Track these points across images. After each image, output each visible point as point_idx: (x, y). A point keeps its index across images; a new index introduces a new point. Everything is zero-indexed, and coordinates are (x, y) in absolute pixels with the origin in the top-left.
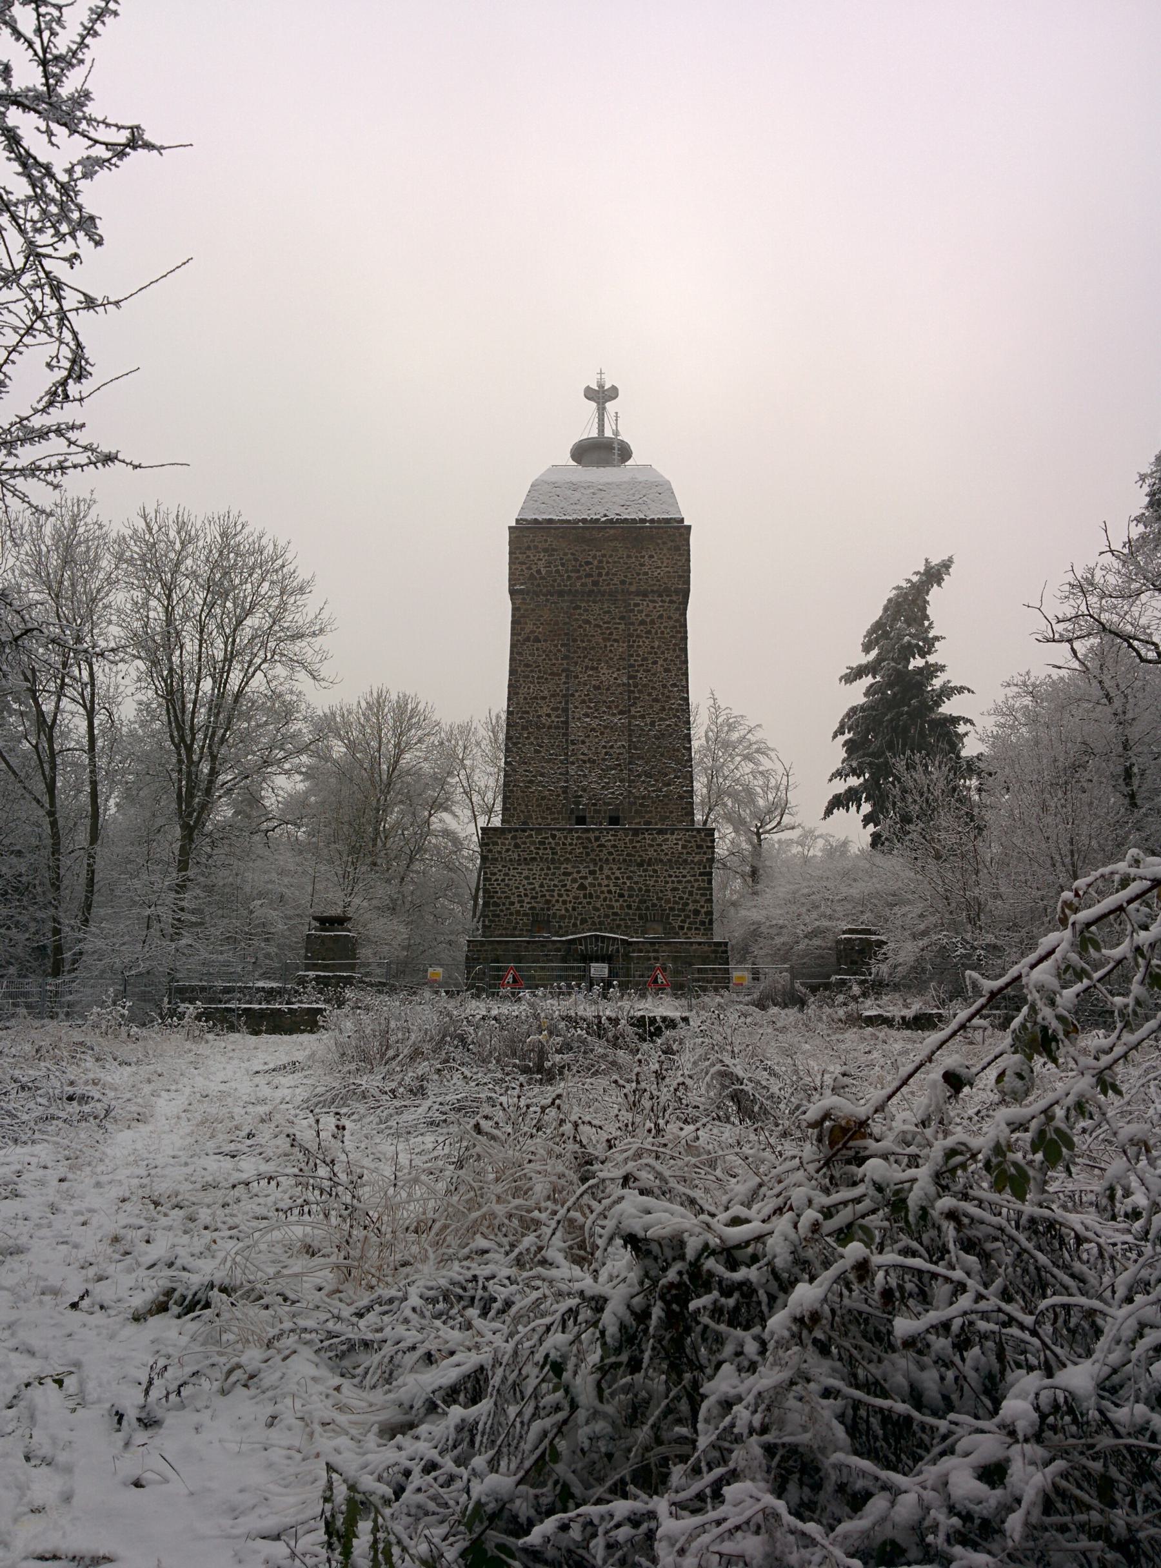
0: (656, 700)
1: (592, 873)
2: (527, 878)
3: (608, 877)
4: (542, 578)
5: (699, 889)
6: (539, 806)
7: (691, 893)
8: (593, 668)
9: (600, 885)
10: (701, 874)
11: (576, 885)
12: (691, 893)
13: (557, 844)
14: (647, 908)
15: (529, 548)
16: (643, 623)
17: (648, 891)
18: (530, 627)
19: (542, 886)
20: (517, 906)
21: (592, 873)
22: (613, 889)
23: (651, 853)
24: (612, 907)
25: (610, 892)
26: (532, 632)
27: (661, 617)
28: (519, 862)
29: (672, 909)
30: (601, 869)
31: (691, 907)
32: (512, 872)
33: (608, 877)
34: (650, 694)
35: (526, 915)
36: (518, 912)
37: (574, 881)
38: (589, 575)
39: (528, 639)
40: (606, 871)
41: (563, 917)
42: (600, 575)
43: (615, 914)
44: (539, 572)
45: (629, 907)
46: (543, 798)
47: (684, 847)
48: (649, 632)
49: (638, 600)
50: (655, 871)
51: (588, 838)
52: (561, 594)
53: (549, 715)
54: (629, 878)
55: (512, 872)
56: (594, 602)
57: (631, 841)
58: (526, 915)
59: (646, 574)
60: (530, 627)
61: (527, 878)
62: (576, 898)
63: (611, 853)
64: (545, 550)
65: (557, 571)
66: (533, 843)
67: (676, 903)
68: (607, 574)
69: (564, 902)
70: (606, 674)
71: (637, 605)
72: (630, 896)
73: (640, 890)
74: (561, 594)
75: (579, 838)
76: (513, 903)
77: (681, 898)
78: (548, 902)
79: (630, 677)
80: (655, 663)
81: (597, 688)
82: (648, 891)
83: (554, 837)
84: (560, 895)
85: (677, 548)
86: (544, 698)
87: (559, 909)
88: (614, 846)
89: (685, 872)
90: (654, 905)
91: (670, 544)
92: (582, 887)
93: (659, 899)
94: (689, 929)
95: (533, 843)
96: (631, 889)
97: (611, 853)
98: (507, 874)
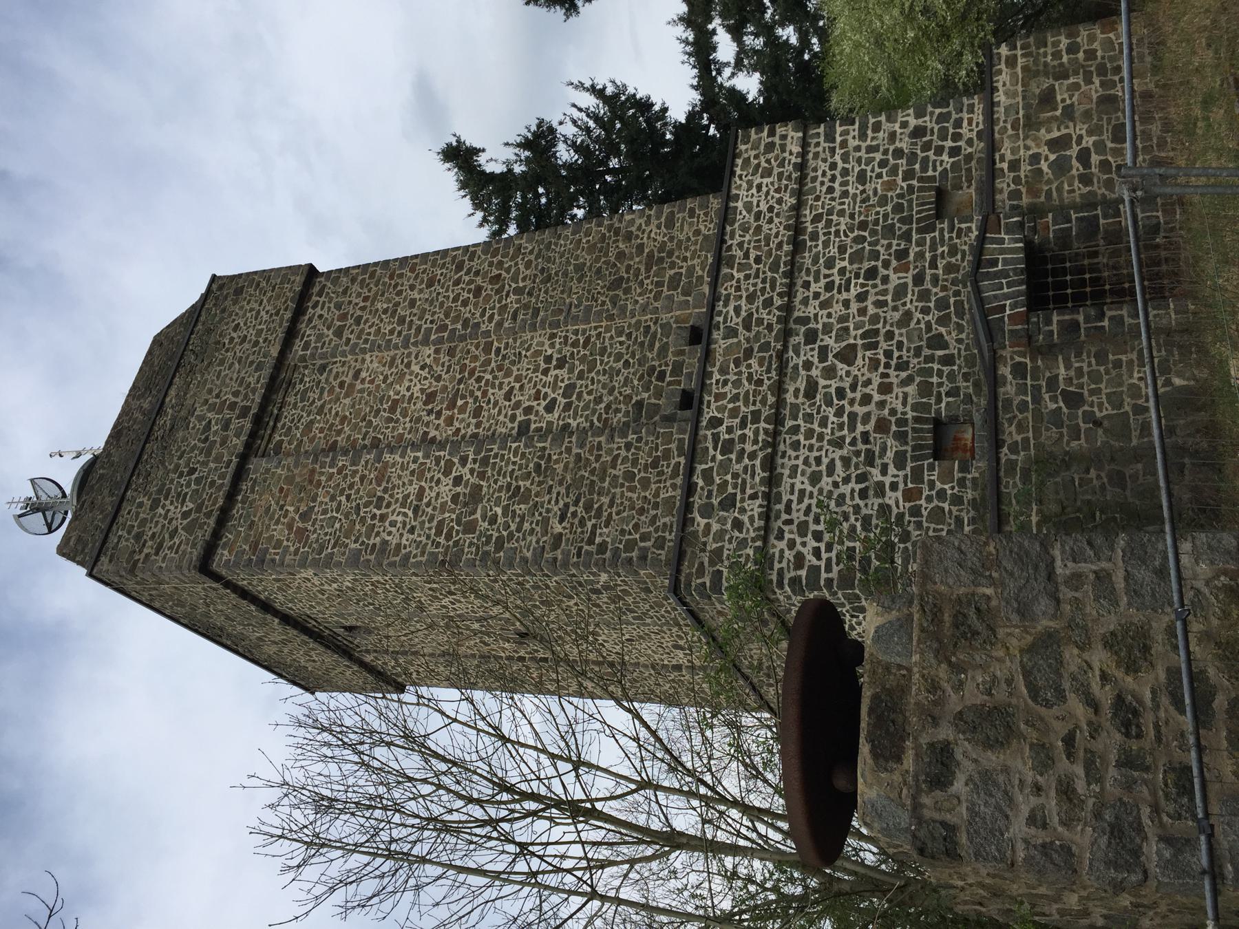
0: (478, 291)
1: (811, 337)
2: (815, 479)
3: (825, 305)
4: (199, 509)
5: (863, 136)
6: (645, 483)
7: (871, 149)
8: (392, 409)
9: (843, 319)
10: (830, 137)
11: (842, 368)
12: (871, 149)
13: (734, 413)
14: (907, 220)
15: (138, 537)
16: (339, 333)
17: (863, 226)
18: (279, 532)
19: (838, 443)
20: (891, 498)
21: (811, 337)
22: (854, 292)
23: (778, 229)
24: (900, 291)
25: (861, 297)
26: (290, 526)
27: (338, 306)
28: (770, 498)
29: (909, 175)
30: (804, 321)
31: (904, 144)
32: (798, 516)
33: (823, 305)
34: (465, 303)
35: (917, 475)
36: (909, 495)
37: (830, 373)
38: (226, 427)
39: (302, 534)
40: (811, 310)
41: (925, 389)
42: (233, 406)
43: (918, 279)
44: (185, 515)
45: (902, 254)
46: (630, 476)
47: (768, 173)
48: (358, 321)
49: (298, 345)
50: (817, 219)
51: (728, 351)
52: (240, 474)
53: (458, 481)
54: (830, 264)
55: (798, 516)
56: (277, 419)
57: (741, 268)
58: (917, 475)
59: (259, 332)
60: (279, 532)
61: (815, 479)
62: (874, 364)
63: (768, 303)
64: (155, 504)
65: (198, 481)
66: (724, 467)
67: (894, 171)
68: (236, 394)
69: (885, 388)
70: (414, 386)
71: (306, 347)
72: (875, 255)
73: (859, 240)
74: (240, 474)
75: (723, 371)
76: (884, 510)
77: (883, 164)
78: (882, 426)
79: (426, 342)
80: (412, 303)
81: (430, 398)
82: (863, 226)
83: (715, 422)
84: (866, 399)
85: (239, 291)
86: (421, 494)
87: (902, 400)
88: (751, 298)
89: (823, 166)
90: (898, 208)
91: (228, 303)
92: (847, 356)
93: (883, 201)
94: (957, 137)
95: (724, 467)
96: (856, 257)
97: (768, 303)
98: (803, 529)
